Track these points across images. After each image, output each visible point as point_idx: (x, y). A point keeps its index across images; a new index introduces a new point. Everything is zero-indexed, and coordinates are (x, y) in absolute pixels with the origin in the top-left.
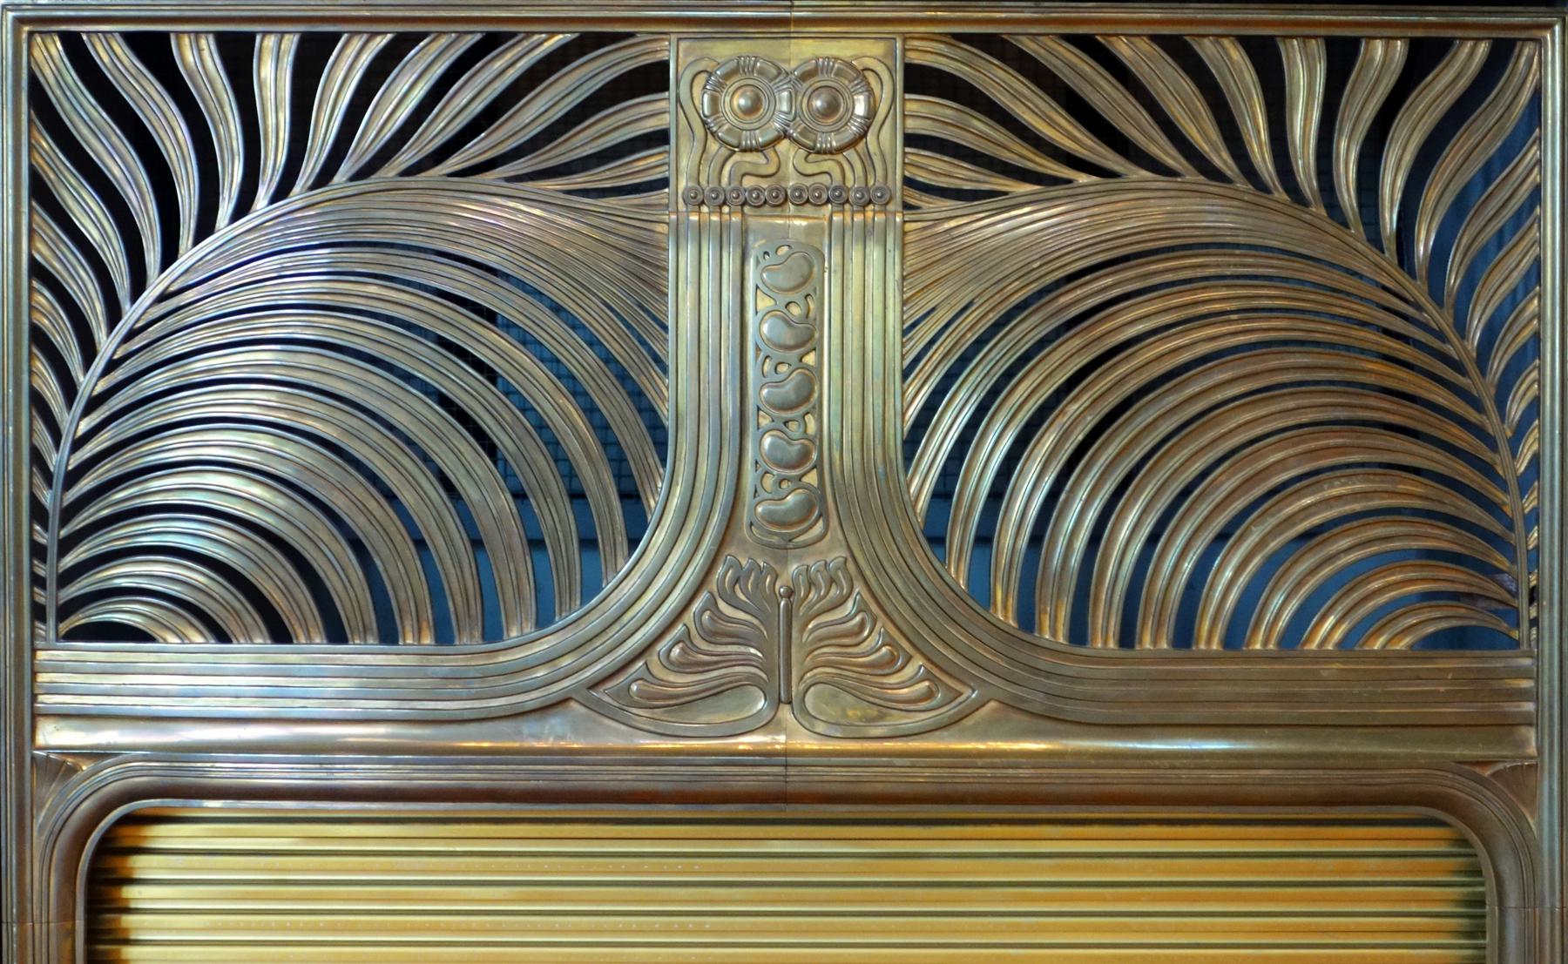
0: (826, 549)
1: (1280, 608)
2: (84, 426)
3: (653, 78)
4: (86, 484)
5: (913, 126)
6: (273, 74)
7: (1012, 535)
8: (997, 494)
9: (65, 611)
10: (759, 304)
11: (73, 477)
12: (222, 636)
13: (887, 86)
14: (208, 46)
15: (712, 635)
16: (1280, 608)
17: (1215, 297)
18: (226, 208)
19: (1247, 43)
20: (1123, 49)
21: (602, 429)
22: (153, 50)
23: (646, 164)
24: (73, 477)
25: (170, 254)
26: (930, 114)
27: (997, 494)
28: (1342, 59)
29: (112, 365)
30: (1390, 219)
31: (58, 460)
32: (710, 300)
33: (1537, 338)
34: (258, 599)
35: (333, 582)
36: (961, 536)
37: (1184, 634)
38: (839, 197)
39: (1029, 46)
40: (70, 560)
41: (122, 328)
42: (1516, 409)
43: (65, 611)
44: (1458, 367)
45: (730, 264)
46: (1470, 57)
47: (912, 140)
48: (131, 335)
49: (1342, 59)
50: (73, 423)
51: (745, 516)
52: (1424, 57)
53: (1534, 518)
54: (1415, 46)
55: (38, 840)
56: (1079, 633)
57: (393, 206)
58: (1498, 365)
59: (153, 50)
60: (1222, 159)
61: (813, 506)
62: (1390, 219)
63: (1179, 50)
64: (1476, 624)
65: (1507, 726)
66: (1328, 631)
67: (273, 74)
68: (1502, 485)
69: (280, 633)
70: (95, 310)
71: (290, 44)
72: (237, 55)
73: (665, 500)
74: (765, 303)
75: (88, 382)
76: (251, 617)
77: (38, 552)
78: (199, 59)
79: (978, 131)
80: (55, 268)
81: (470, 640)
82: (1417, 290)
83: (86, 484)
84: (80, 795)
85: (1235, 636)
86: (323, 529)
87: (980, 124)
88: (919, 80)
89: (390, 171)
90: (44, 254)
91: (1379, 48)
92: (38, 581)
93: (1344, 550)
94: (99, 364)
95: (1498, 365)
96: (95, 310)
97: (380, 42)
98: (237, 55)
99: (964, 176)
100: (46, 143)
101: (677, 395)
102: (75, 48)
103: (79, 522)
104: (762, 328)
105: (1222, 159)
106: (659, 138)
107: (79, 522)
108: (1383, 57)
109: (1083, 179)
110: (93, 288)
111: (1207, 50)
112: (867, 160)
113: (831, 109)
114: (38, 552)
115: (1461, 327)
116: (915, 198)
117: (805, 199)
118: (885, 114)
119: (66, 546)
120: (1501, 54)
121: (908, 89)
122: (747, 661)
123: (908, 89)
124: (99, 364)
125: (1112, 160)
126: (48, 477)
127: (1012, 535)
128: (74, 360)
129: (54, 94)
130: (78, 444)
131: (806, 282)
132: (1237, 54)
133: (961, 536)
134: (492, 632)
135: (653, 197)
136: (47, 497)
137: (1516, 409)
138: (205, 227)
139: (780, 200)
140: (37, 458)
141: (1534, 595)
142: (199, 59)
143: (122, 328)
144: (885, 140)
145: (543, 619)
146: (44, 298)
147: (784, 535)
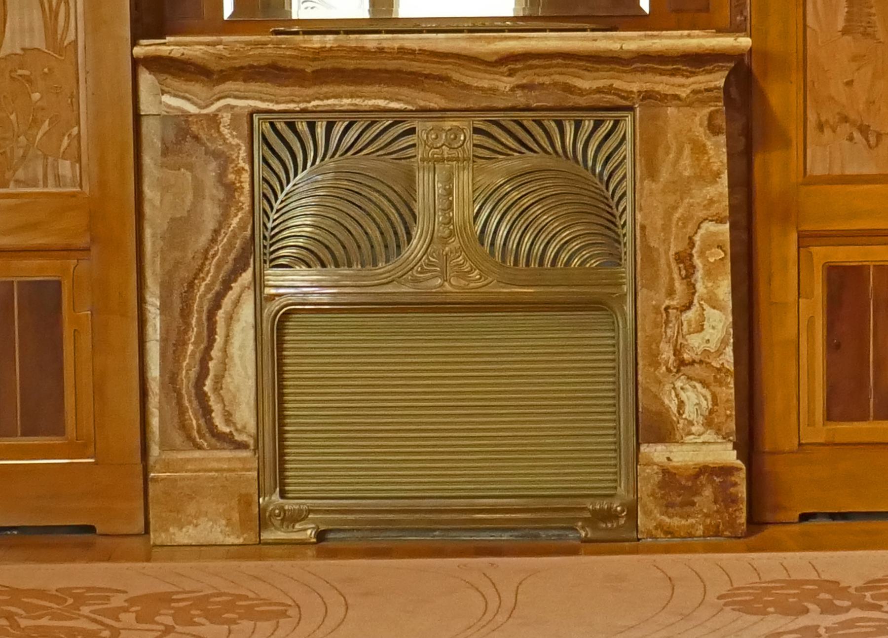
0: (455, 243)
1: (564, 257)
2: (276, 217)
3: (412, 131)
4: (276, 230)
5: (475, 142)
6: (320, 131)
7: (499, 241)
8: (495, 232)
9: (272, 261)
10: (438, 185)
11: (273, 229)
12: (309, 266)
13: (469, 132)
14: (304, 124)
15: (428, 265)
16: (564, 257)
17: (548, 183)
18: (309, 164)
19: (555, 121)
20: (525, 123)
21: (401, 215)
22: (291, 126)
23: (410, 152)
24: (273, 229)
25: (296, 175)
26: (478, 139)
27: (495, 232)
28: (578, 124)
29: (282, 202)
30: (590, 163)
31: (270, 225)
32: (428, 186)
33: (625, 192)
34: (313, 257)
35: (336, 253)
36: (488, 240)
37: (541, 263)
38: (457, 159)
39: (503, 123)
40: (272, 249)
41: (285, 193)
42: (621, 209)
43: (272, 261)
44: (607, 199)
45: (431, 175)
46: (609, 125)
47: (475, 145)
48: (287, 194)
49: (578, 124)
50: (273, 216)
51: (435, 235)
52: (598, 124)
53: (625, 235)
54: (595, 121)
55: (265, 315)
56: (516, 262)
57: (349, 162)
58: (616, 199)
59: (291, 126)
60: (550, 149)
61: (451, 234)
62: (590, 163)
63: (539, 123)
64: (616, 259)
65: (622, 284)
66: (576, 262)
67: (320, 131)
68: (616, 226)
69: (323, 265)
70: (277, 187)
71: (325, 123)
72: (312, 126)
73: (416, 232)
74: (440, 185)
75: (276, 206)
76: (318, 262)
77: (265, 247)
78: (302, 127)
79: (489, 143)
80: (268, 178)
81: (357, 267)
82: (597, 181)
83: (276, 230)
84: (275, 306)
85: (554, 262)
86: (335, 241)
87: (491, 141)
88: (476, 131)
89: (349, 153)
90: (266, 175)
91: (587, 123)
92: (265, 254)
93: (575, 245)
94: (279, 201)
95: (616, 199)
96: (277, 187)
97: (346, 123)
98: (312, 126)
99: (487, 154)
100: (265, 148)
101: (418, 208)
102: (272, 125)
103: (274, 240)
104: (439, 191)
105: (550, 149)
106: (414, 145)
107: (274, 240)
108: (588, 125)
109: (516, 154)
110: (278, 183)
111: (546, 123)
112: (464, 151)
113: (456, 137)
114: (265, 247)
115: (607, 188)
116: (476, 159)
117: (449, 160)
118: (467, 138)
119: (271, 245)
120: (616, 123)
121: (474, 133)
122: (435, 271)
123: (474, 133)
124: (279, 201)
125: (523, 150)
126: (267, 228)
127: (499, 241)
128: (273, 201)
129: (267, 136)
130: (274, 220)
131: (450, 179)
132: (553, 124)
133: (488, 240)
134: (375, 264)
135: (413, 160)
136: (267, 234)
137: (621, 209)
138: (304, 168)
139: (443, 160)
140: (264, 224)
141: (625, 253)
142: (302, 127)
143: (285, 193)
144: (468, 145)
145: (387, 261)
146: (266, 186)
147: (444, 241)
